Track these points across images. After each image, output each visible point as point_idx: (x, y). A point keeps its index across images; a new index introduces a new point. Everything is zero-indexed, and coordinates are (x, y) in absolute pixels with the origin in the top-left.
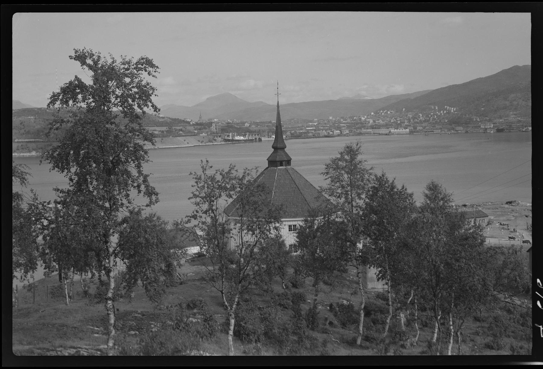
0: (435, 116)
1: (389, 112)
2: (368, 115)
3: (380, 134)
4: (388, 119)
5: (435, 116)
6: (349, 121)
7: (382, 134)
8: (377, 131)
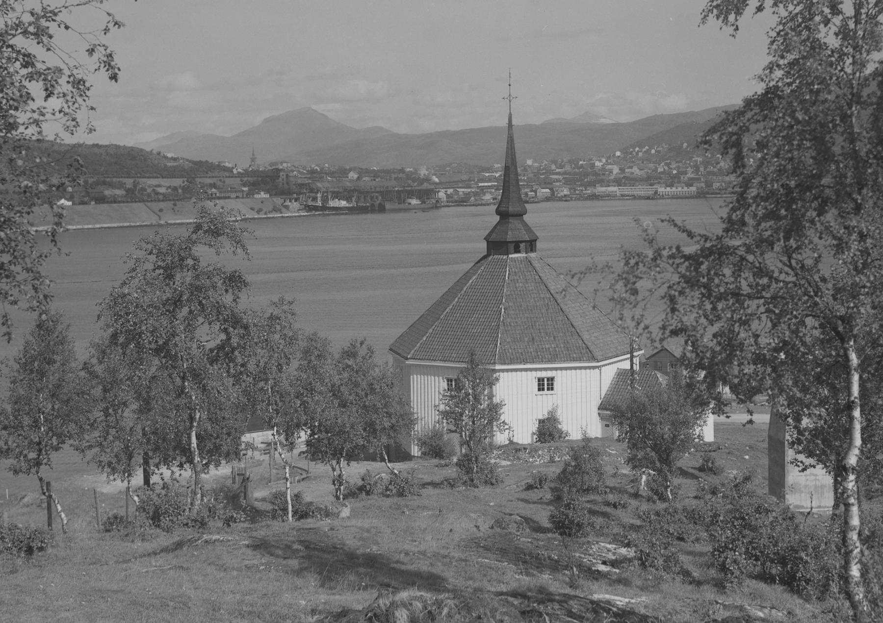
0: (752, 160)
1: (653, 151)
2: (609, 158)
3: (634, 197)
4: (651, 165)
5: (752, 160)
6: (568, 168)
7: (640, 198)
8: (627, 190)
